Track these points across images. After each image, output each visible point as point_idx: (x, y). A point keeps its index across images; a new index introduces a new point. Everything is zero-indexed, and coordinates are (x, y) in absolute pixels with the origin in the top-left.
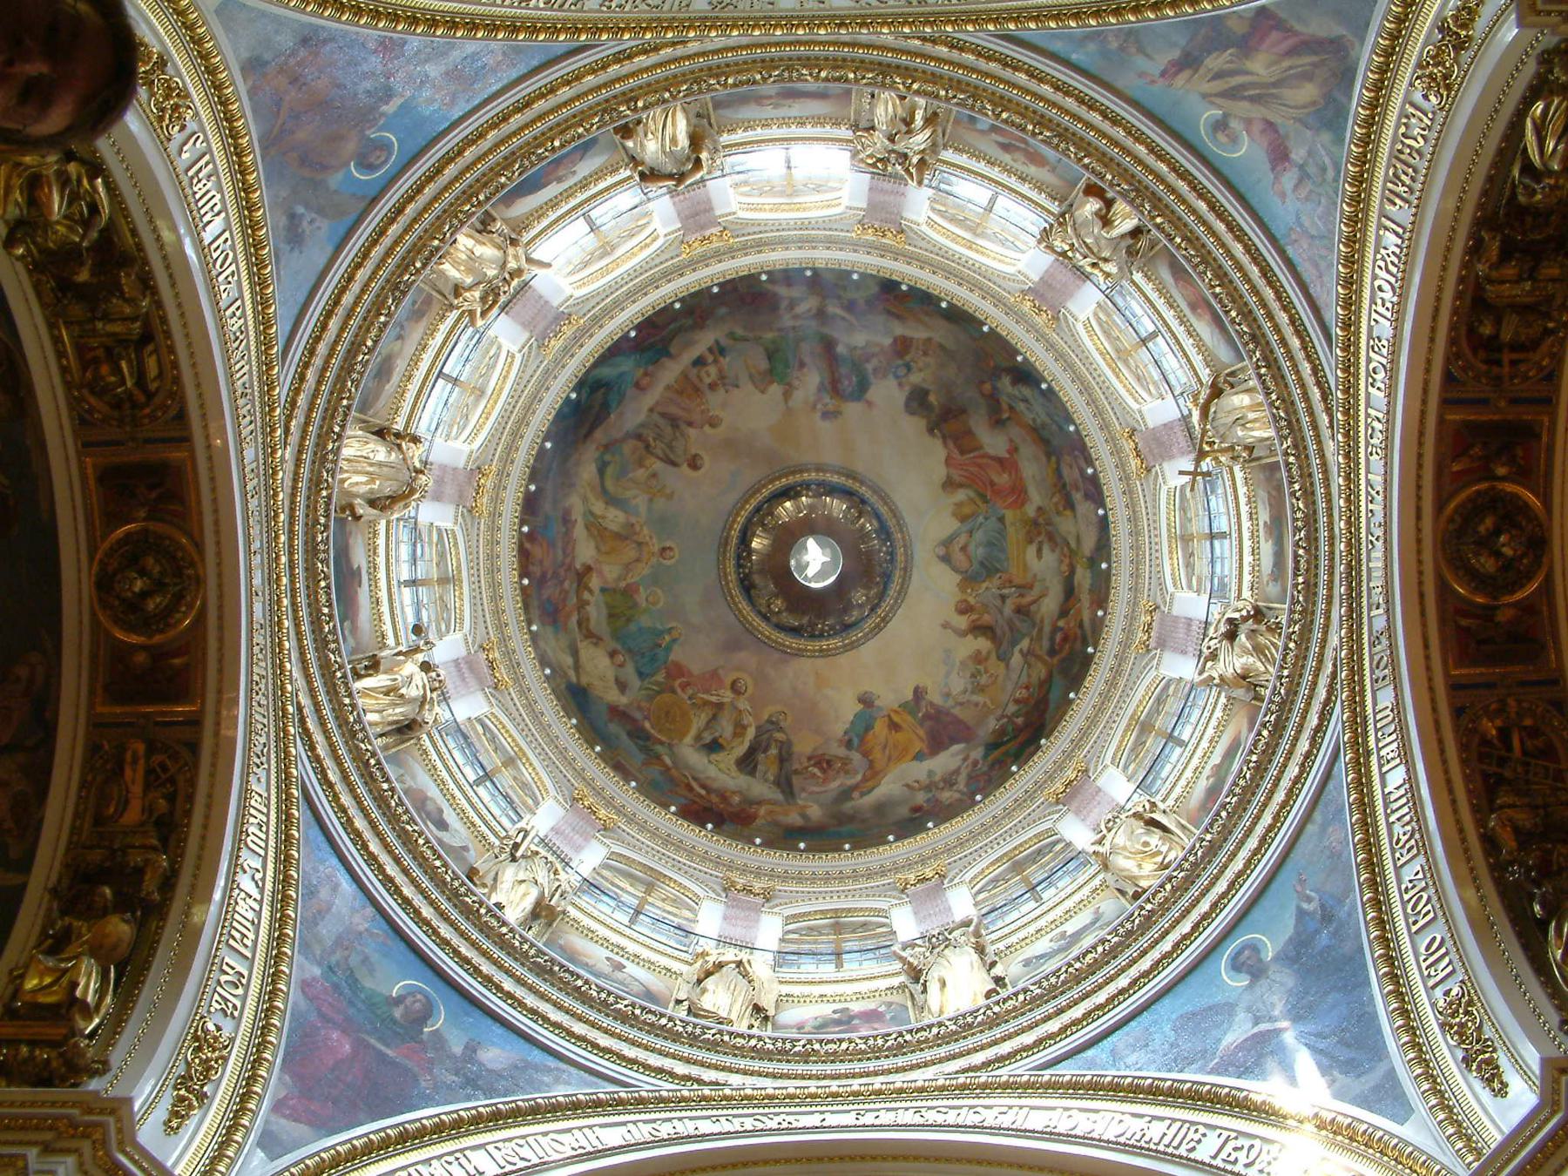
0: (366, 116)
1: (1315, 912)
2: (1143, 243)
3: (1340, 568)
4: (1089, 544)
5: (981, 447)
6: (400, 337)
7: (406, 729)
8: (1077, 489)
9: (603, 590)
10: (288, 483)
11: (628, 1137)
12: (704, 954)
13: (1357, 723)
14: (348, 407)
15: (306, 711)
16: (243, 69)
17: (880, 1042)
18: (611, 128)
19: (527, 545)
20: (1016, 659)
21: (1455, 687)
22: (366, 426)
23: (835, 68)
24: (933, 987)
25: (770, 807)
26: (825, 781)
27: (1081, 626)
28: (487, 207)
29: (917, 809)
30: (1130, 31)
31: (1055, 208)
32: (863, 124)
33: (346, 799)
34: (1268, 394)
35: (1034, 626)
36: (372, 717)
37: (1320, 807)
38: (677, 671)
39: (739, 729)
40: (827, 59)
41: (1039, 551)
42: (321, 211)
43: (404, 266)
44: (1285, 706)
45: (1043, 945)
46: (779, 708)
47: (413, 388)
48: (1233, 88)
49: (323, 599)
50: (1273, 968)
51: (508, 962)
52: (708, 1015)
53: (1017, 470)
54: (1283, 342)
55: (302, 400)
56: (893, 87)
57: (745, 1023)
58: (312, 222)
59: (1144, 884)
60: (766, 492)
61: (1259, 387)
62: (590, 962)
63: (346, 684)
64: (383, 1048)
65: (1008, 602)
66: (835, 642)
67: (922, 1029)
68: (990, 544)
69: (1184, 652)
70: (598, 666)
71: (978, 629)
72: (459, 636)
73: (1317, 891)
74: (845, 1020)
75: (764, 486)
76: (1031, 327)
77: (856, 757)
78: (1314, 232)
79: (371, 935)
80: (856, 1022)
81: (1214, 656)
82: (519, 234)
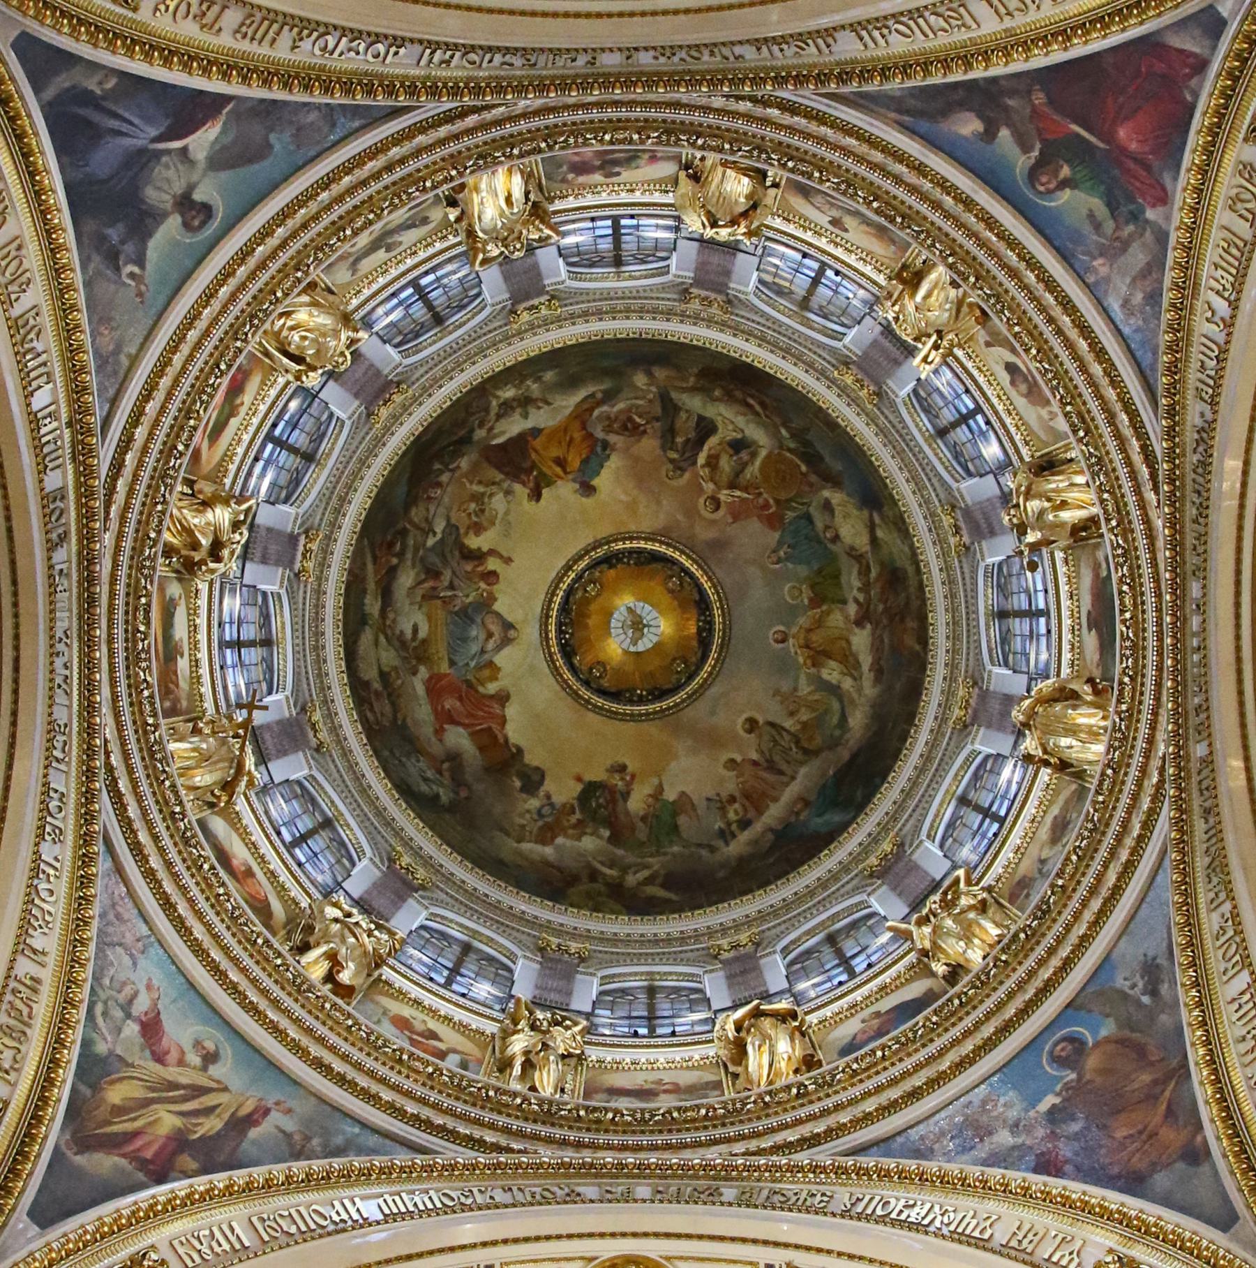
0: (1074, 1093)
1: (125, 264)
2: (298, 938)
3: (102, 610)
4: (367, 637)
5: (473, 735)
6: (1043, 862)
7: (1047, 466)
8: (377, 694)
9: (844, 602)
10: (1163, 719)
11: (830, 40)
12: (750, 234)
13: (82, 454)
14: (1098, 793)
15: (1149, 486)
16: (1208, 1153)
17: (572, 140)
18: (826, 1068)
19: (917, 647)
20: (439, 527)
22: (1080, 775)
23: (598, 1121)
24: (518, 194)
26: (629, 410)
27: (375, 559)
28: (952, 992)
30: (297, 1155)
31: (386, 973)
32: (573, 1061)
33: (1111, 394)
34: (173, 786)
35: (422, 560)
36: (1080, 479)
38: (773, 521)
39: (712, 462)
40: (606, 1131)
41: (415, 630)
42: (1124, 996)
43: (1034, 936)
44: (162, 476)
46: (674, 483)
47: (1030, 809)
48: (194, 1098)
49: (1128, 601)
50: (169, 206)
51: (947, 226)
52: (745, 171)
53: (435, 711)
54: (156, 838)
55: (1146, 803)
56: (541, 1102)
57: (709, 163)
58: (1133, 986)
59: (305, 298)
60: (683, 694)
61: (183, 792)
62: (864, 227)
63: (1106, 512)
65: (446, 584)
66: (620, 546)
67: (529, 153)
68: (465, 640)
69: (269, 530)
70: (851, 529)
71: (478, 556)
72: (989, 561)
74: (608, 165)
75: (683, 701)
76: (417, 853)
77: (600, 434)
78: (119, 950)
79: (1088, 253)
80: (598, 163)
81: (236, 525)
82: (919, 961)
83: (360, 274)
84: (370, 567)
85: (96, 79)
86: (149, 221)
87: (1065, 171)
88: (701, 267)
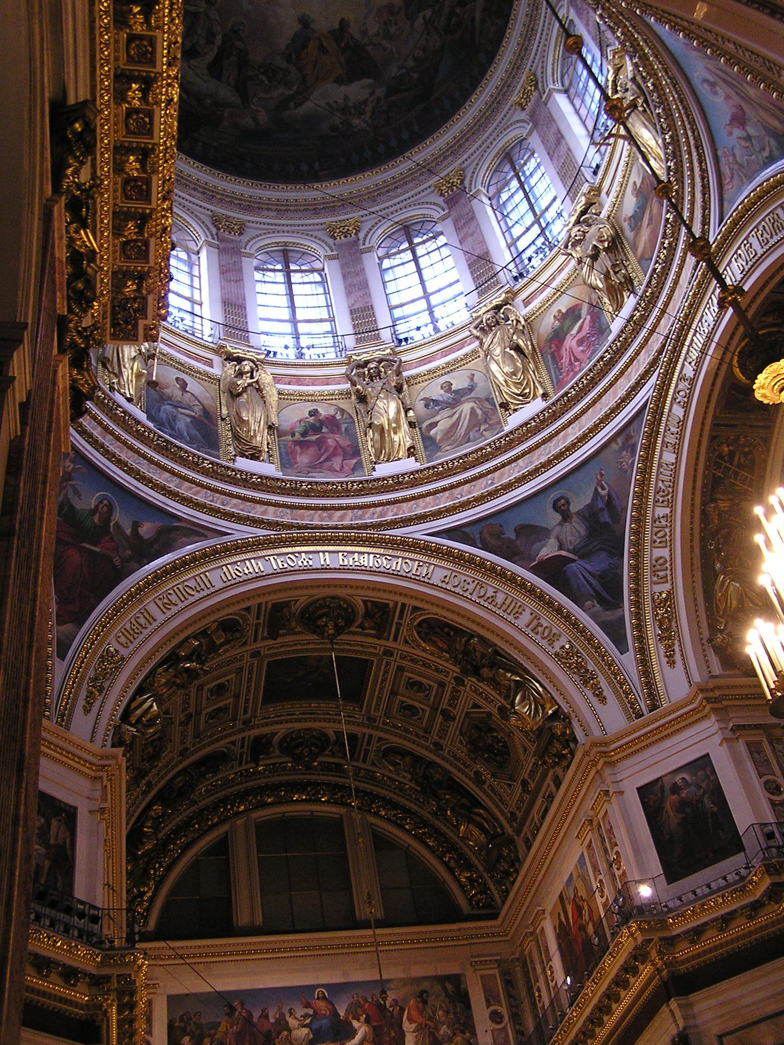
11: (225, 579)
20: (419, 23)
21: (715, 425)
25: (231, 109)
27: (473, 19)
29: (334, 128)
37: (623, 436)
39: (210, 37)
45: (435, 391)
50: (575, 519)
51: (144, 449)
62: (168, 391)
64: (93, 548)
73: (609, 486)
77: (293, 69)
80: (324, 430)
83: (468, 373)
84: (478, 15)
85: (595, 609)
86: (587, 515)
87: (96, 518)
88: (240, 280)
